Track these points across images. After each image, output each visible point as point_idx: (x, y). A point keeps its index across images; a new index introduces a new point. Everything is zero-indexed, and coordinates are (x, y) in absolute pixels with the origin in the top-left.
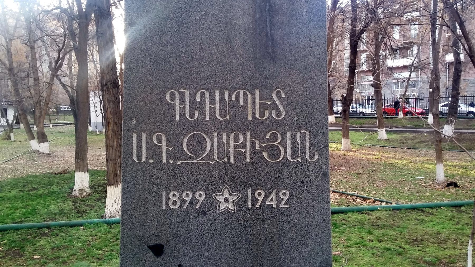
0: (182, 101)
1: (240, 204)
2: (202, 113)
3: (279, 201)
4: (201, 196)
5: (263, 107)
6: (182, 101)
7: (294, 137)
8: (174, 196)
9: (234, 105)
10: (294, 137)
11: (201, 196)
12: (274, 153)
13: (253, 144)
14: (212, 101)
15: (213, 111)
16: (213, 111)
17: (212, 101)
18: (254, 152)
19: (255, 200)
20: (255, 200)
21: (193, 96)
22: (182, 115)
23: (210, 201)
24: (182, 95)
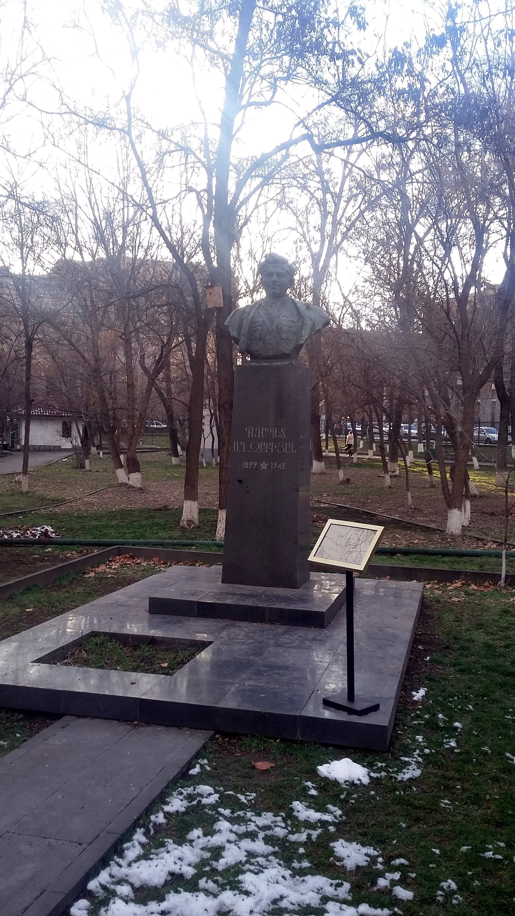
0: (251, 431)
1: (269, 467)
2: (257, 435)
3: (282, 467)
4: (255, 464)
5: (278, 434)
6: (251, 431)
7: (288, 444)
8: (246, 463)
9: (269, 433)
10: (288, 444)
11: (255, 464)
12: (281, 449)
13: (274, 447)
14: (261, 431)
15: (261, 434)
16: (261, 434)
17: (261, 431)
18: (274, 449)
19: (274, 466)
20: (274, 466)
21: (254, 429)
22: (251, 435)
23: (258, 465)
24: (251, 429)
